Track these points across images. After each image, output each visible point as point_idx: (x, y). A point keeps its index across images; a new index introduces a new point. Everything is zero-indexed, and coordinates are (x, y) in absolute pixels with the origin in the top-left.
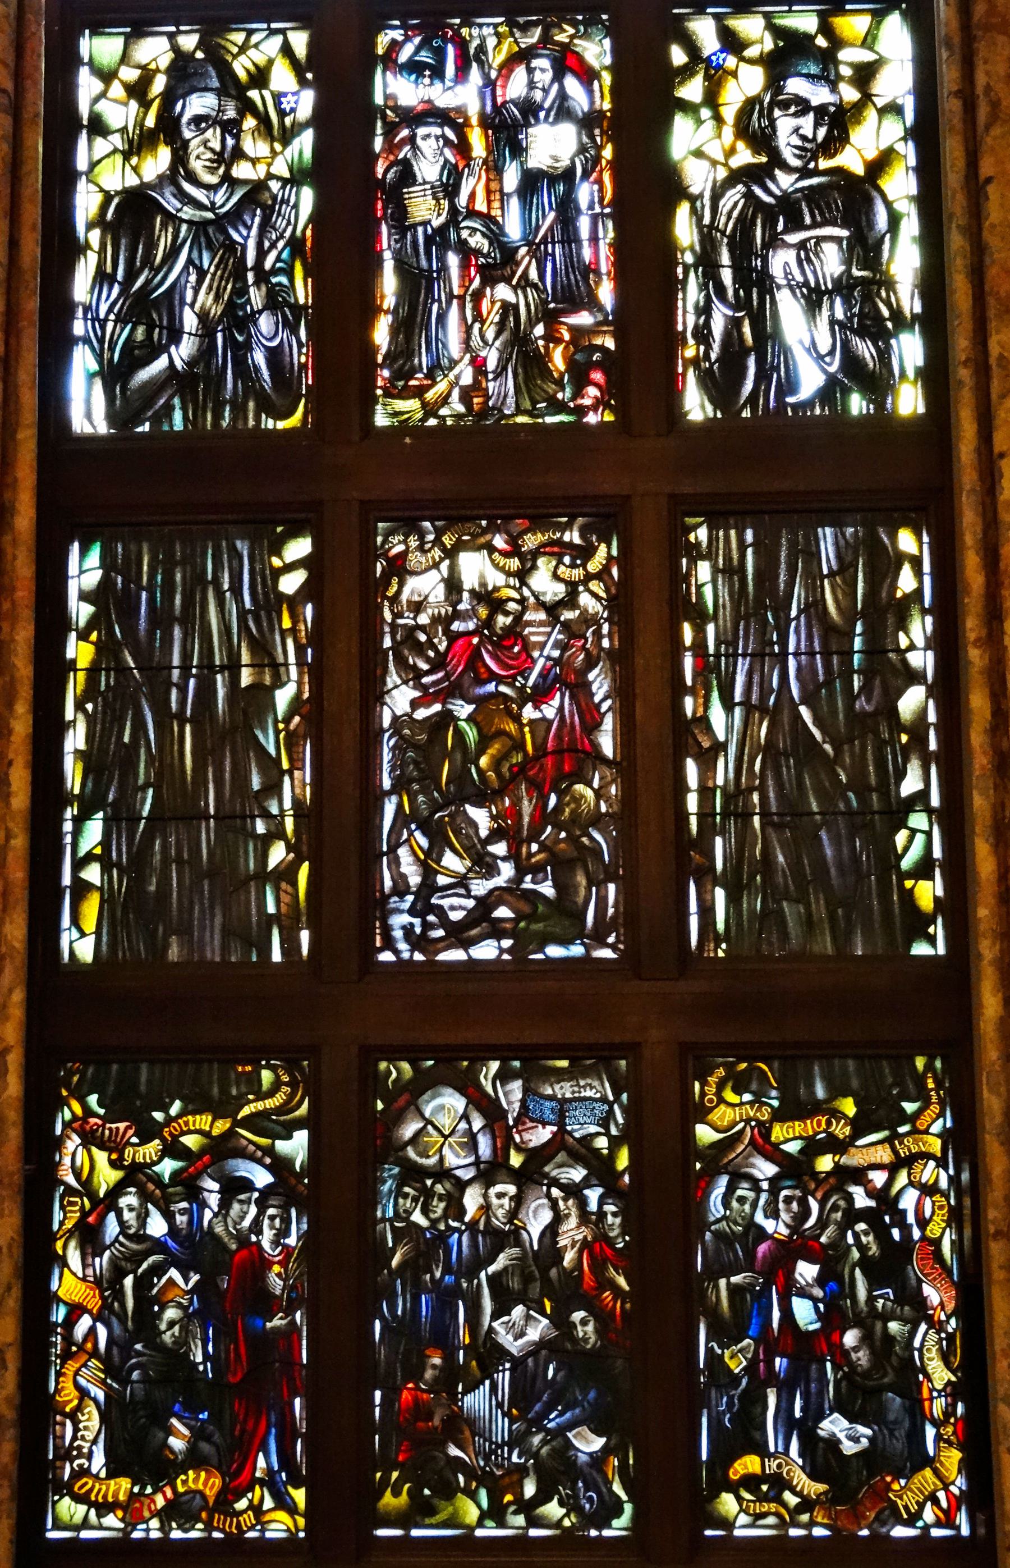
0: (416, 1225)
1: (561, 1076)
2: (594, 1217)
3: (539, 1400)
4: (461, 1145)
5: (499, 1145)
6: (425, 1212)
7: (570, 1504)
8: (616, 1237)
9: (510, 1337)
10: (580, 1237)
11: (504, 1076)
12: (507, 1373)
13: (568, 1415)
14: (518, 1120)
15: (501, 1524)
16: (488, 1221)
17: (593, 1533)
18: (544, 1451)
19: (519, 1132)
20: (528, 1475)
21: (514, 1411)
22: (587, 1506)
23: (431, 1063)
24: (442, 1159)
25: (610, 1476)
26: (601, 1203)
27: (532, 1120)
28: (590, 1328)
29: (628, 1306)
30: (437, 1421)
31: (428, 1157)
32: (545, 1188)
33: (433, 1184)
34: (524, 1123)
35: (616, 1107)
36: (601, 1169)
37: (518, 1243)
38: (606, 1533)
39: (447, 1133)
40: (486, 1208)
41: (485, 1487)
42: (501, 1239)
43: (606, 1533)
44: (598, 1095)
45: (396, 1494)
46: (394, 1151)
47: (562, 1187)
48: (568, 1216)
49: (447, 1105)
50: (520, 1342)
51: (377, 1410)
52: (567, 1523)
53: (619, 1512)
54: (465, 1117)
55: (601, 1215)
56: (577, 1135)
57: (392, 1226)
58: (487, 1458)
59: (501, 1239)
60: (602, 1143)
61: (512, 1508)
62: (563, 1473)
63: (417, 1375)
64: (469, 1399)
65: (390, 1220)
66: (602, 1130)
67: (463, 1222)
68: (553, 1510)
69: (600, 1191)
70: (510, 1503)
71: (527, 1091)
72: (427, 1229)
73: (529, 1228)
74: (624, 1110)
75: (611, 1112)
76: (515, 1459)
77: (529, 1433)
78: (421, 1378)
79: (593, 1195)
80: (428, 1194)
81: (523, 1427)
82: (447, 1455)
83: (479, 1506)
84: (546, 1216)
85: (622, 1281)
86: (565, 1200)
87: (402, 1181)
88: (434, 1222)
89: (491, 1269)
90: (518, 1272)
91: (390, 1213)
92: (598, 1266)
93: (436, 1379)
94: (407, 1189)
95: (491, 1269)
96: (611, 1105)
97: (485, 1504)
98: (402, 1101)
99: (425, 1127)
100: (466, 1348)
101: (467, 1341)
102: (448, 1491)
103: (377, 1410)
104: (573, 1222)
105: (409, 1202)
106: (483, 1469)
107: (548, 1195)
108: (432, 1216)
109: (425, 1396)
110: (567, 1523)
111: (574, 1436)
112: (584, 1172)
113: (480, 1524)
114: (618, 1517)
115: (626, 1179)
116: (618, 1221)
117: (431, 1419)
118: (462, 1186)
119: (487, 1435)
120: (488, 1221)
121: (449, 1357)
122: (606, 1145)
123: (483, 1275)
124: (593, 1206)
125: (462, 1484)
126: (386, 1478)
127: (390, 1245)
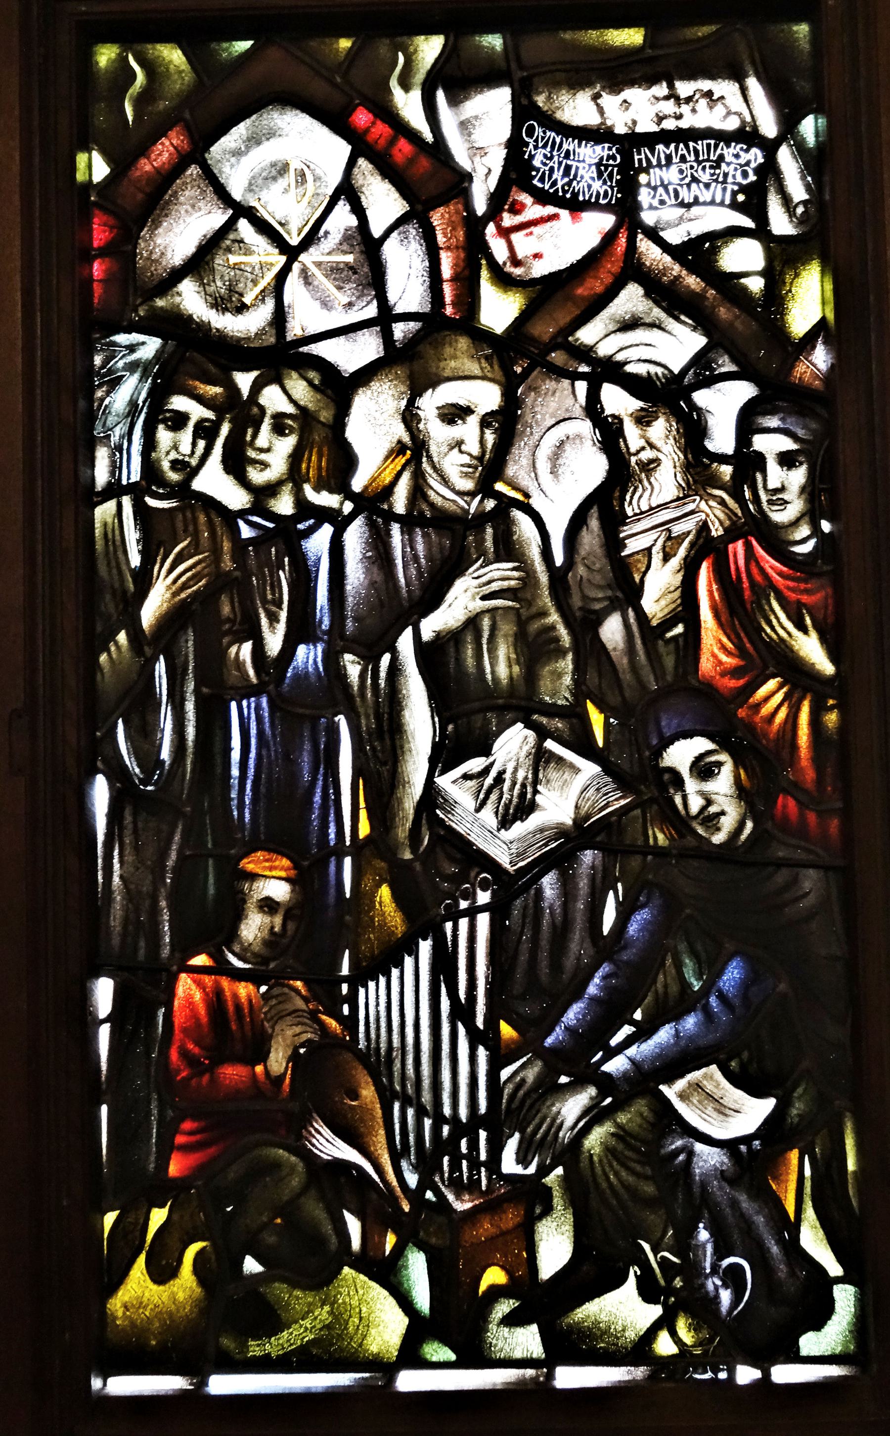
0: (210, 504)
1: (618, 72)
2: (726, 470)
3: (578, 994)
4: (335, 271)
5: (447, 271)
6: (236, 464)
7: (680, 1295)
8: (795, 523)
9: (488, 817)
10: (689, 525)
11: (456, 79)
12: (483, 921)
13: (664, 1035)
14: (499, 200)
15: (473, 1354)
16: (418, 491)
17: (746, 1375)
18: (595, 1140)
19: (505, 233)
20: (548, 1210)
21: (506, 1030)
22: (726, 1296)
23: (243, 46)
24: (280, 317)
25: (790, 1207)
26: (747, 423)
27: (542, 197)
28: (723, 784)
29: (832, 718)
30: (278, 1060)
31: (241, 308)
32: (582, 387)
33: (257, 387)
34: (517, 209)
35: (785, 157)
36: (745, 332)
37: (508, 549)
38: (784, 1374)
39: (294, 241)
40: (414, 450)
41: (421, 1247)
42: (457, 539)
43: (784, 1374)
44: (732, 124)
45: (162, 1273)
46: (141, 295)
47: (635, 385)
48: (649, 467)
49: (288, 159)
50: (519, 829)
51: (104, 1032)
52: (664, 1346)
53: (820, 1315)
54: (347, 191)
55: (748, 463)
56: (674, 237)
57: (141, 510)
58: (427, 1166)
59: (457, 539)
60: (744, 258)
61: (504, 1307)
62: (650, 1203)
63: (220, 930)
64: (372, 997)
65: (133, 490)
66: (747, 222)
67: (349, 495)
68: (624, 1309)
69: (743, 391)
70: (496, 1293)
71: (524, 112)
72: (242, 514)
73: (536, 502)
74: (813, 162)
75: (769, 170)
76: (509, 1164)
77: (546, 1088)
78: (231, 935)
79: (723, 404)
80: (245, 414)
81: (531, 1075)
82: (310, 1158)
83: (405, 1302)
84: (589, 468)
85: (811, 649)
86: (643, 420)
87: (165, 378)
88: (262, 495)
89: (431, 625)
90: (507, 628)
91: (134, 473)
92: (741, 610)
93: (273, 941)
94: (179, 403)
95: (431, 625)
96: (770, 148)
97: (422, 1299)
98: (164, 152)
99: (229, 226)
100: (359, 849)
101: (364, 829)
102: (317, 1263)
103: (104, 1032)
104: (666, 482)
105: (186, 437)
106: (415, 1196)
107: (593, 409)
108: (257, 477)
109: (244, 990)
110: (664, 1346)
111: (682, 1096)
112: (698, 341)
113: (410, 1356)
114: (818, 1326)
115: (821, 357)
116: (798, 477)
117: (263, 1057)
118: (340, 388)
119: (426, 1097)
120: (418, 491)
121: (309, 876)
122: (759, 263)
123: (405, 643)
124: (722, 438)
125: (356, 1243)
126: (129, 1236)
127: (135, 560)
